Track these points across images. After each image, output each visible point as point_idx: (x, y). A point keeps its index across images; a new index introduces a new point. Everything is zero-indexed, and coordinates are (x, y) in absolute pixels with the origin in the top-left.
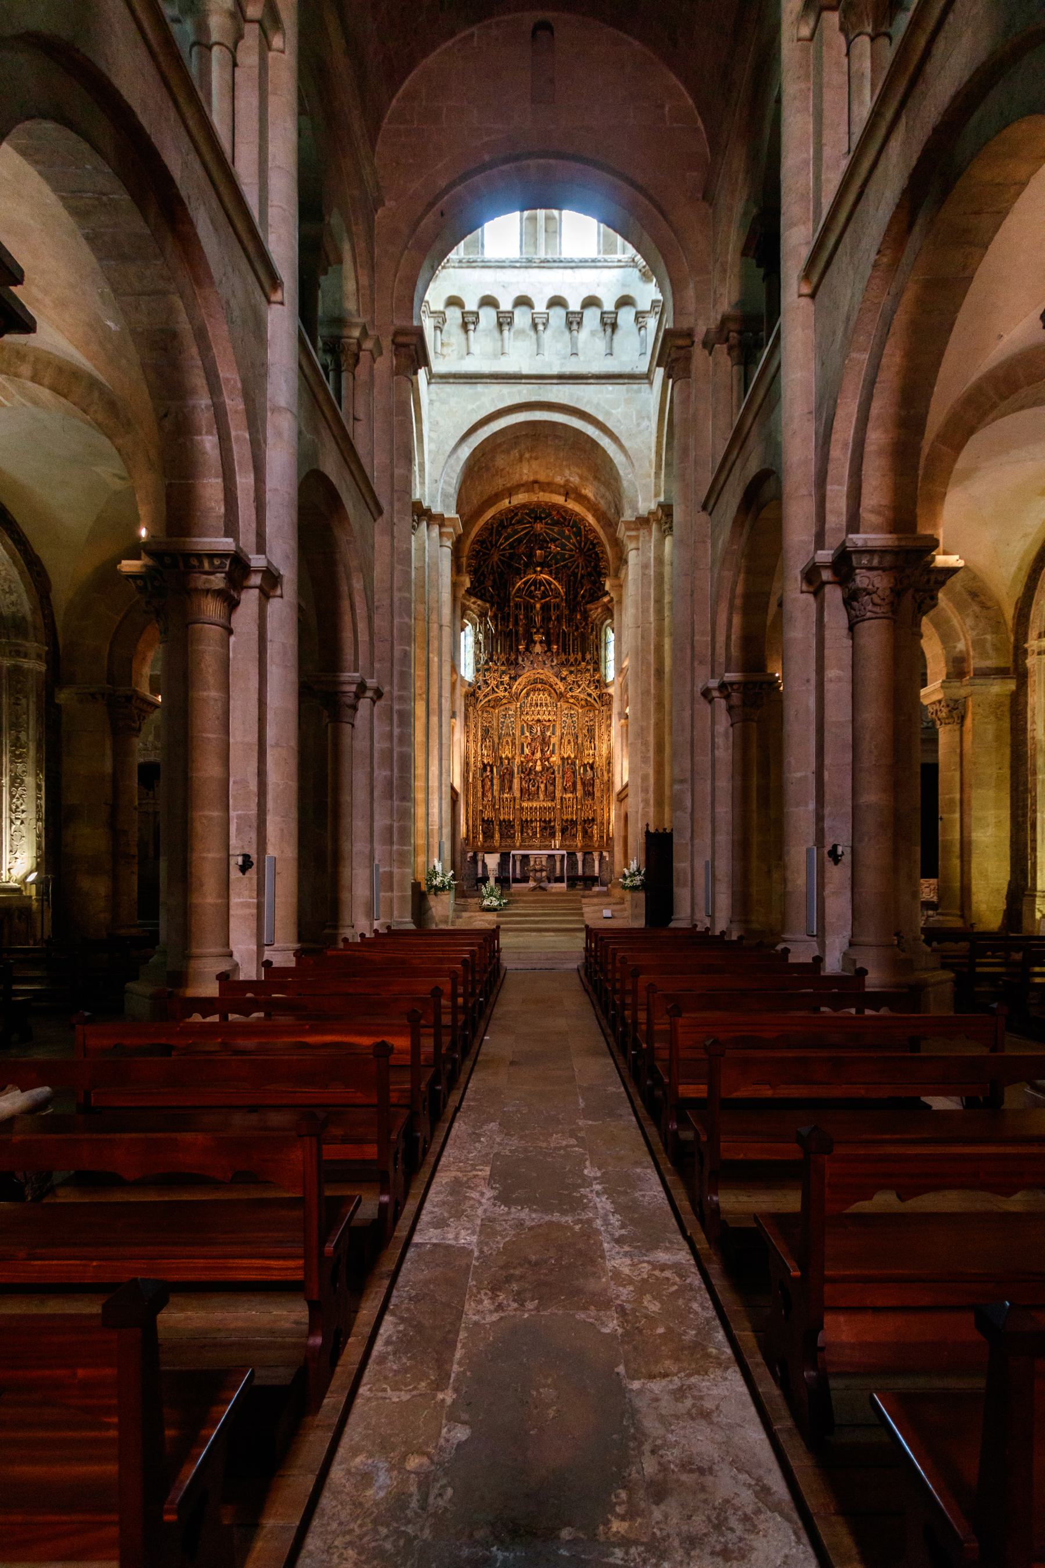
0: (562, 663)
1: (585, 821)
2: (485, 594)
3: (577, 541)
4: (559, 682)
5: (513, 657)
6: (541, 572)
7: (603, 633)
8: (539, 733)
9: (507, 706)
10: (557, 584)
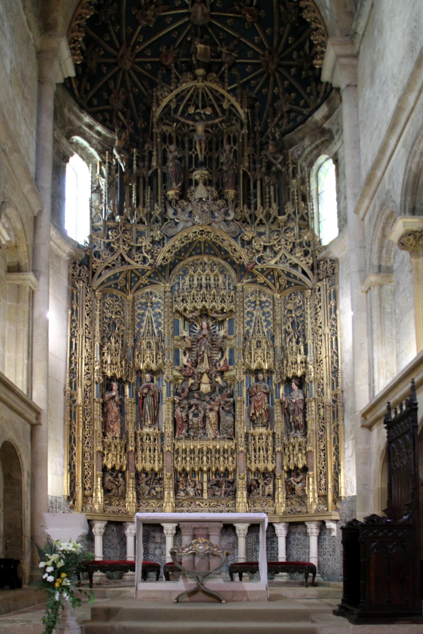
0: (245, 221)
1: (289, 472)
4: (238, 247)
5: (158, 210)
8: (205, 332)
9: (147, 290)
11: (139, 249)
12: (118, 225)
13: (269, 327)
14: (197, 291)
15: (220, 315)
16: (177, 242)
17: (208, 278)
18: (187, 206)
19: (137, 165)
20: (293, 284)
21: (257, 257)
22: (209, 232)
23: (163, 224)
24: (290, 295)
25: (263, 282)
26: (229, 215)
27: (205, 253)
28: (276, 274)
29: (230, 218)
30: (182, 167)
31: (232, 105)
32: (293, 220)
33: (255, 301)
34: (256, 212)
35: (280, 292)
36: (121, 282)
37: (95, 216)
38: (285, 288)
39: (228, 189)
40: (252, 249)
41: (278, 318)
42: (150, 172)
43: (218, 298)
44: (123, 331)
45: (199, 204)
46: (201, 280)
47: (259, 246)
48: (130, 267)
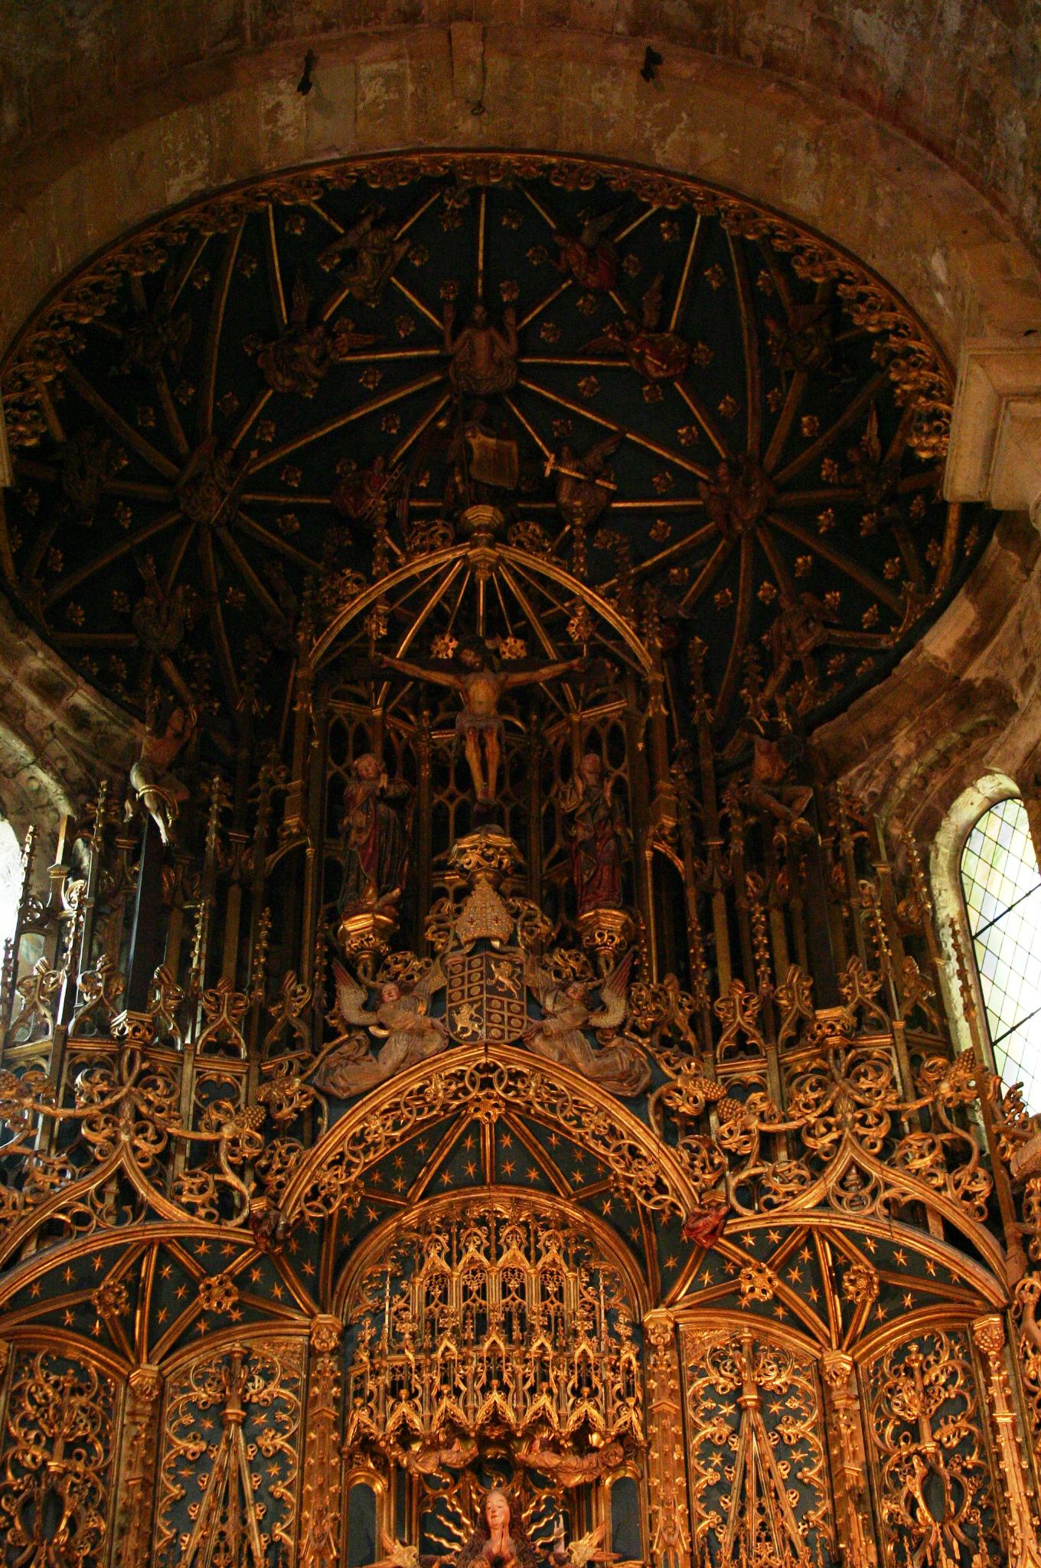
2: (131, 687)
3: (720, 424)
4: (649, 1141)
5: (299, 995)
6: (499, 536)
7: (942, 882)
8: (500, 1543)
10: (607, 611)
11: (204, 1155)
12: (121, 1053)
13: (814, 1516)
14: (462, 1343)
15: (573, 1461)
16: (375, 1123)
17: (513, 1284)
18: (420, 971)
19: (222, 834)
20: (908, 1301)
21: (733, 1183)
22: (516, 1076)
23: (317, 1054)
24: (902, 1352)
25: (768, 1296)
26: (605, 1009)
27: (499, 1180)
28: (826, 1258)
29: (611, 1019)
30: (404, 832)
31: (603, 627)
32: (879, 1026)
33: (739, 1391)
34: (717, 1003)
35: (847, 1338)
36: (110, 1298)
37: (23, 1020)
38: (872, 1325)
39: (598, 907)
40: (711, 1149)
41: (852, 1469)
42: (272, 859)
43: (563, 1374)
44: (96, 1535)
45: (477, 962)
46: (483, 1292)
47: (738, 1137)
48: (155, 1232)
